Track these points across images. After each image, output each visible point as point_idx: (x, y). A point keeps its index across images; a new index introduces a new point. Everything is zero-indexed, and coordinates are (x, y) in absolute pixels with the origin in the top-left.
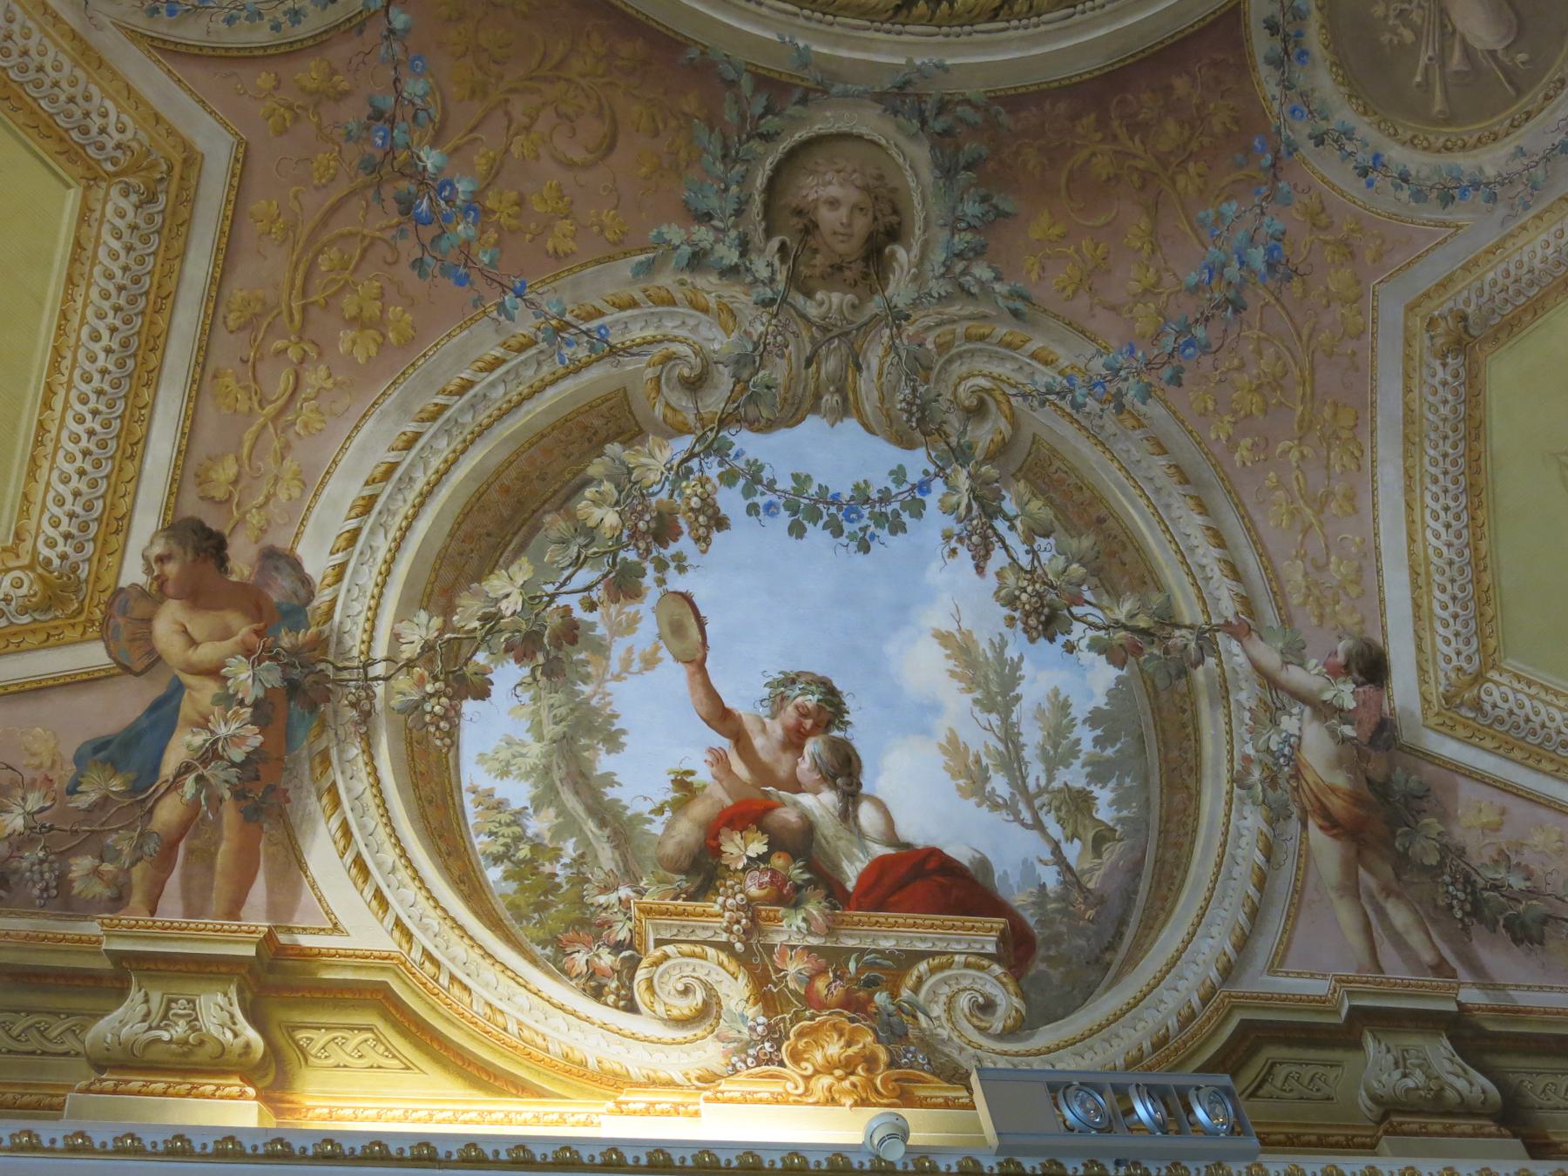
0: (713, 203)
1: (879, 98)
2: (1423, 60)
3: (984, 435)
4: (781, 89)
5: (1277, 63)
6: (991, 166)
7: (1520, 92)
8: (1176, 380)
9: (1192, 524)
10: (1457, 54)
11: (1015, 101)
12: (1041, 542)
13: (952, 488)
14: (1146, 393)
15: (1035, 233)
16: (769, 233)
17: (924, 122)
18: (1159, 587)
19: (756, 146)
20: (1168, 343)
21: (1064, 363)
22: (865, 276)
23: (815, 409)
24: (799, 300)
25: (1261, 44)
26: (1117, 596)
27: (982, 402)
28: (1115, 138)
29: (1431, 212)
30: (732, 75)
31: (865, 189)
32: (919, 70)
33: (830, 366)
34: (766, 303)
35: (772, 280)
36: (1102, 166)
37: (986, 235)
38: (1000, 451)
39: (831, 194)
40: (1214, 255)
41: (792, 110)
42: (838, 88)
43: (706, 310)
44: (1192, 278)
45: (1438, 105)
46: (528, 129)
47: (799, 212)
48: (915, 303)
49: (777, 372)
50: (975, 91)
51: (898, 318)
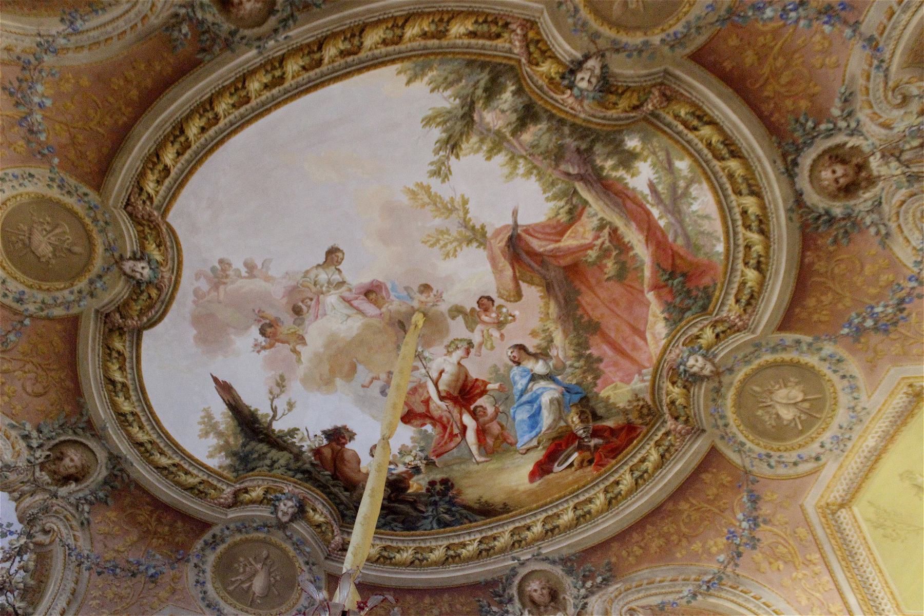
0: (45, 431)
1: (110, 453)
2: (238, 578)
3: (40, 538)
4: (90, 427)
5: (206, 543)
6: (116, 492)
7: (251, 606)
8: (99, 574)
9: (62, 603)
10: (247, 585)
11: (138, 486)
12: (22, 572)
13: (18, 540)
14: (89, 569)
15: (108, 514)
16: (49, 450)
17: (114, 468)
18: (34, 609)
19: (70, 432)
20: (108, 565)
21: (79, 544)
22: (59, 480)
23: (10, 493)
24: (37, 469)
25: (207, 536)
26: (23, 599)
27: (49, 531)
28: (151, 517)
29: (202, 605)
30: (84, 413)
31: (83, 465)
32: (126, 459)
33: (26, 488)
34: (29, 461)
35: (37, 459)
36: (141, 519)
37: (96, 502)
38: (36, 544)
39: (73, 459)
40: (143, 560)
41: (88, 434)
42: (104, 442)
43: (13, 448)
44: (131, 559)
45: (231, 588)
46: (25, 372)
47: (62, 453)
48: (62, 498)
49: (12, 477)
50: (134, 476)
51: (55, 496)
